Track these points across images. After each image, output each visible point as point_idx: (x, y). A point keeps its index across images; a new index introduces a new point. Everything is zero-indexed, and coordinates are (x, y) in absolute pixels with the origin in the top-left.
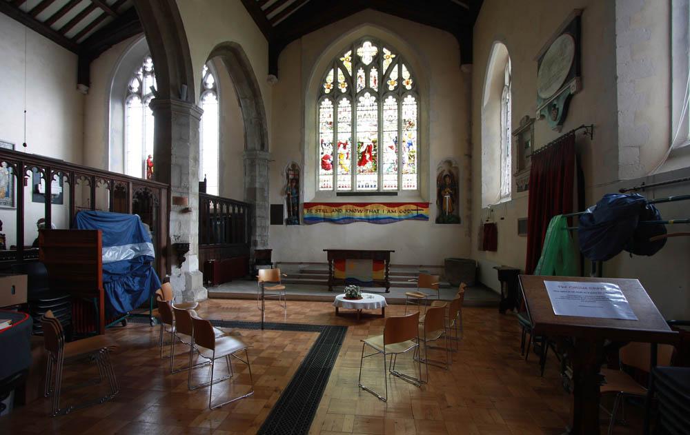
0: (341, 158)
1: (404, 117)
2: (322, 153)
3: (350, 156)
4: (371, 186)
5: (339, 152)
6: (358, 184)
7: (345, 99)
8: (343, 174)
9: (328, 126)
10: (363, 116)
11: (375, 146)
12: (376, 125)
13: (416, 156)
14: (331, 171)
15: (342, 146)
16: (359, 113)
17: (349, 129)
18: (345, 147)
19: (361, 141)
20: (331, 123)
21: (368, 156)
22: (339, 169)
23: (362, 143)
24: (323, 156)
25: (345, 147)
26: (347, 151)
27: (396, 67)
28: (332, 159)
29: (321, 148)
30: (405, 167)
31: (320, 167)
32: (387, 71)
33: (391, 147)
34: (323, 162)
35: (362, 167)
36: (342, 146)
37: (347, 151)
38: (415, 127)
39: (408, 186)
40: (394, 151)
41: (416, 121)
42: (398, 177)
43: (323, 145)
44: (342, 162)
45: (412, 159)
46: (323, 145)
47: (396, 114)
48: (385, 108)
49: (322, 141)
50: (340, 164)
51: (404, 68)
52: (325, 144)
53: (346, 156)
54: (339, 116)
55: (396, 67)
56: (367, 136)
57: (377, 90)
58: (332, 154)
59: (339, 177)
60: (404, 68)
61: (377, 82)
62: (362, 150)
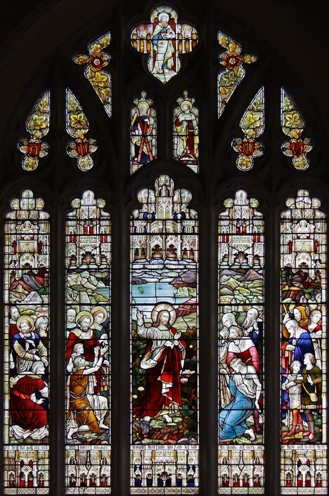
0: (79, 389)
1: (287, 260)
2: (13, 373)
3: (107, 385)
4: (179, 483)
5: (70, 368)
6: (133, 474)
7: (88, 196)
8: (84, 442)
9: (31, 282)
10: (149, 253)
11: (190, 353)
12: (192, 285)
13: (324, 389)
14: (42, 432)
15: (80, 348)
16: (137, 241)
17: (106, 294)
18: (89, 355)
19: (141, 331)
20: (42, 270)
21: (166, 387)
22: (72, 427)
23: (149, 341)
24: (14, 381)
25: (89, 355)
26: (98, 363)
27: (259, 97)
28: (45, 391)
29: (8, 357)
30: (288, 421)
31: (7, 415)
32: (229, 107)
33: (244, 357)
34: (14, 400)
35: (147, 418)
36: (80, 348)
37: (98, 363)
38: (322, 297)
39: (300, 484)
40: (251, 369)
41: (323, 276)
42: (266, 455)
43: (16, 345)
44: (79, 403)
45: (313, 397)
46: (16, 345)
47: (260, 251)
48: (224, 227)
49: (14, 329)
50: (73, 407)
51: (285, 102)
52: (22, 342)
53: (93, 382)
54: (71, 250)
55: (259, 97)
56: (164, 318)
57: (195, 168)
58: (44, 377)
59: (71, 452)
60: (285, 102)
61: (197, 140)
62: (147, 364)
